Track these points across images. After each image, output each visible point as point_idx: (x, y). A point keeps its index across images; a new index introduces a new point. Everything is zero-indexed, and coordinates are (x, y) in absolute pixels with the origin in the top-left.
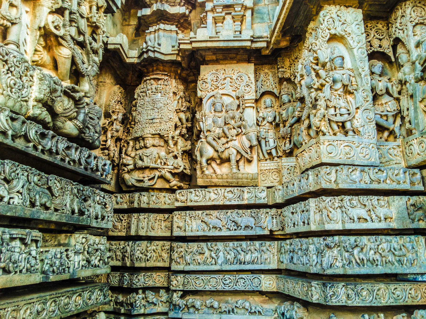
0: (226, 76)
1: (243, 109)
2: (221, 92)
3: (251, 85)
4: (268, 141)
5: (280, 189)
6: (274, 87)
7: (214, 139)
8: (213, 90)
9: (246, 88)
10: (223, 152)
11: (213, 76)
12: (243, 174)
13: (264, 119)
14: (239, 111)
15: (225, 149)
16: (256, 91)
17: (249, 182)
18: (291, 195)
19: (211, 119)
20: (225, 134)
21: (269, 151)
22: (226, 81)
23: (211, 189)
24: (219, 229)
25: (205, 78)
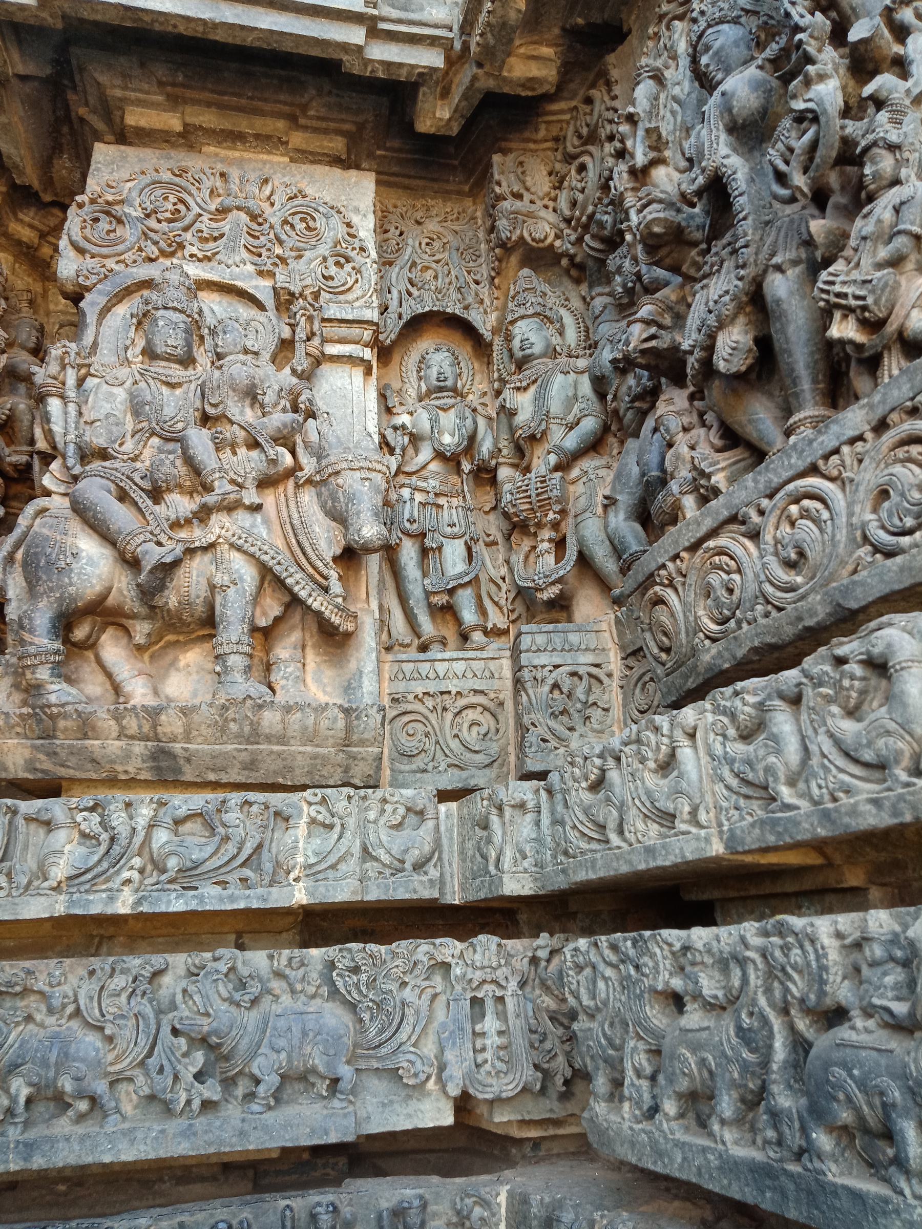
0: (229, 201)
1: (318, 363)
2: (195, 271)
3: (359, 259)
4: (440, 548)
5: (521, 806)
6: (470, 299)
7: (123, 496)
8: (152, 260)
9: (333, 270)
10: (167, 569)
11: (159, 192)
12: (288, 709)
13: (415, 439)
14: (287, 370)
15: (190, 552)
16: (384, 309)
17: (325, 759)
18: (650, 851)
19: (121, 394)
20: (195, 468)
21: (437, 600)
22: (226, 226)
23: (56, 807)
24: (83, 1106)
25: (110, 198)
